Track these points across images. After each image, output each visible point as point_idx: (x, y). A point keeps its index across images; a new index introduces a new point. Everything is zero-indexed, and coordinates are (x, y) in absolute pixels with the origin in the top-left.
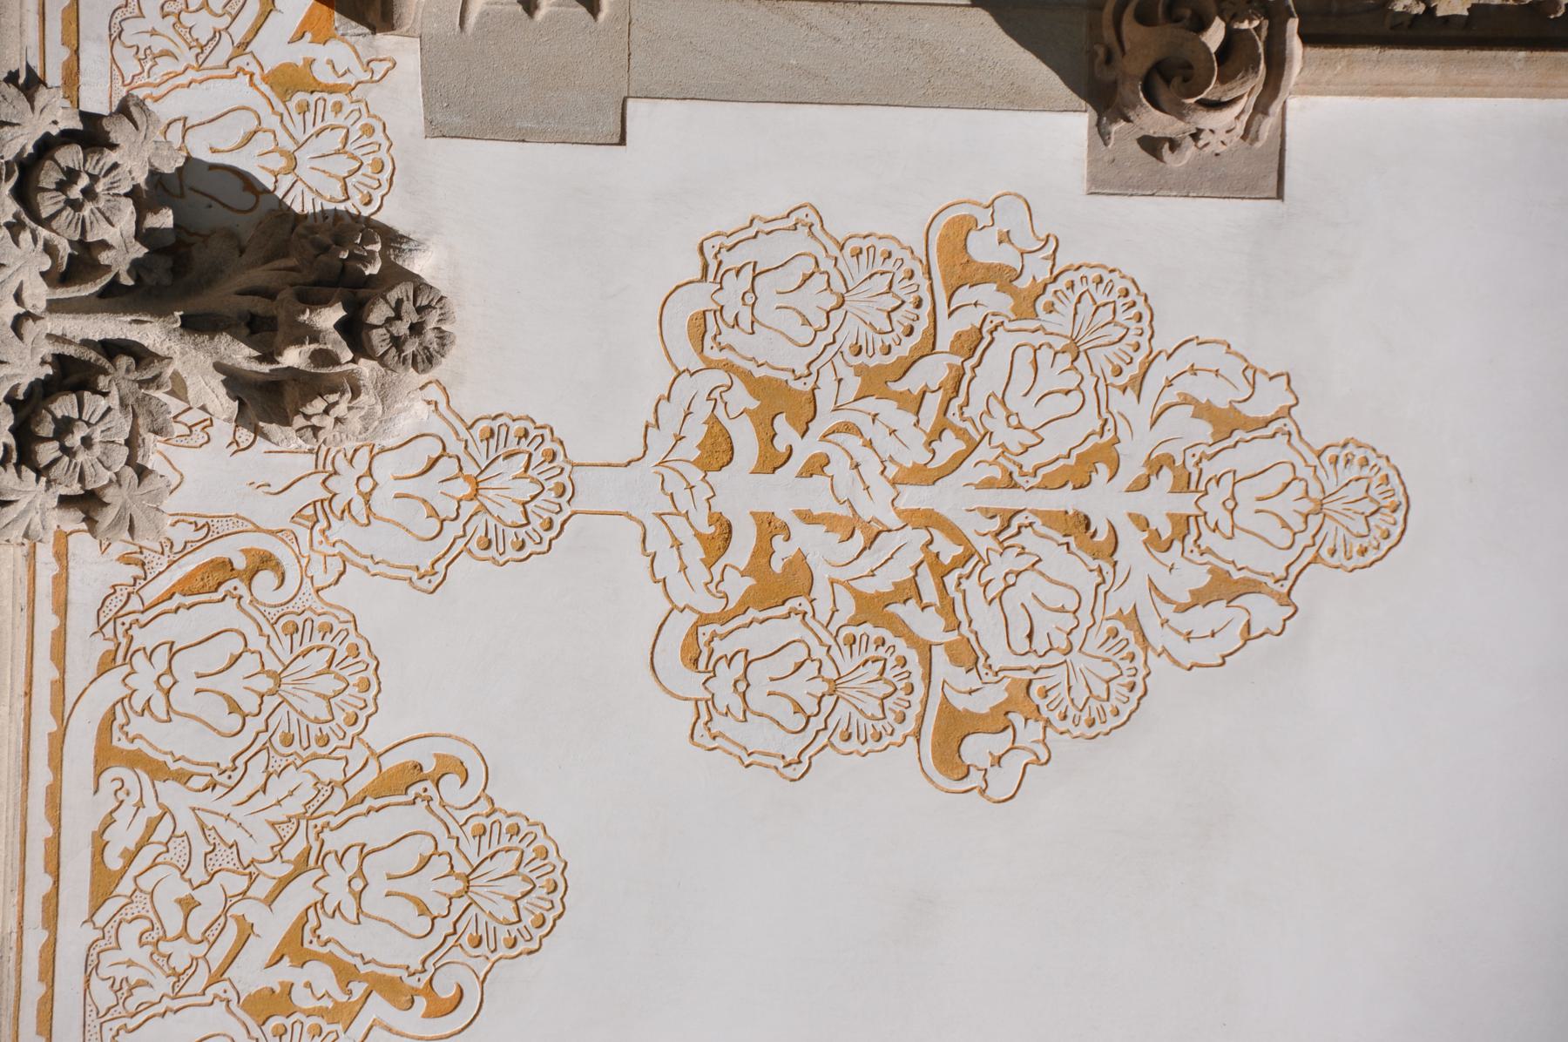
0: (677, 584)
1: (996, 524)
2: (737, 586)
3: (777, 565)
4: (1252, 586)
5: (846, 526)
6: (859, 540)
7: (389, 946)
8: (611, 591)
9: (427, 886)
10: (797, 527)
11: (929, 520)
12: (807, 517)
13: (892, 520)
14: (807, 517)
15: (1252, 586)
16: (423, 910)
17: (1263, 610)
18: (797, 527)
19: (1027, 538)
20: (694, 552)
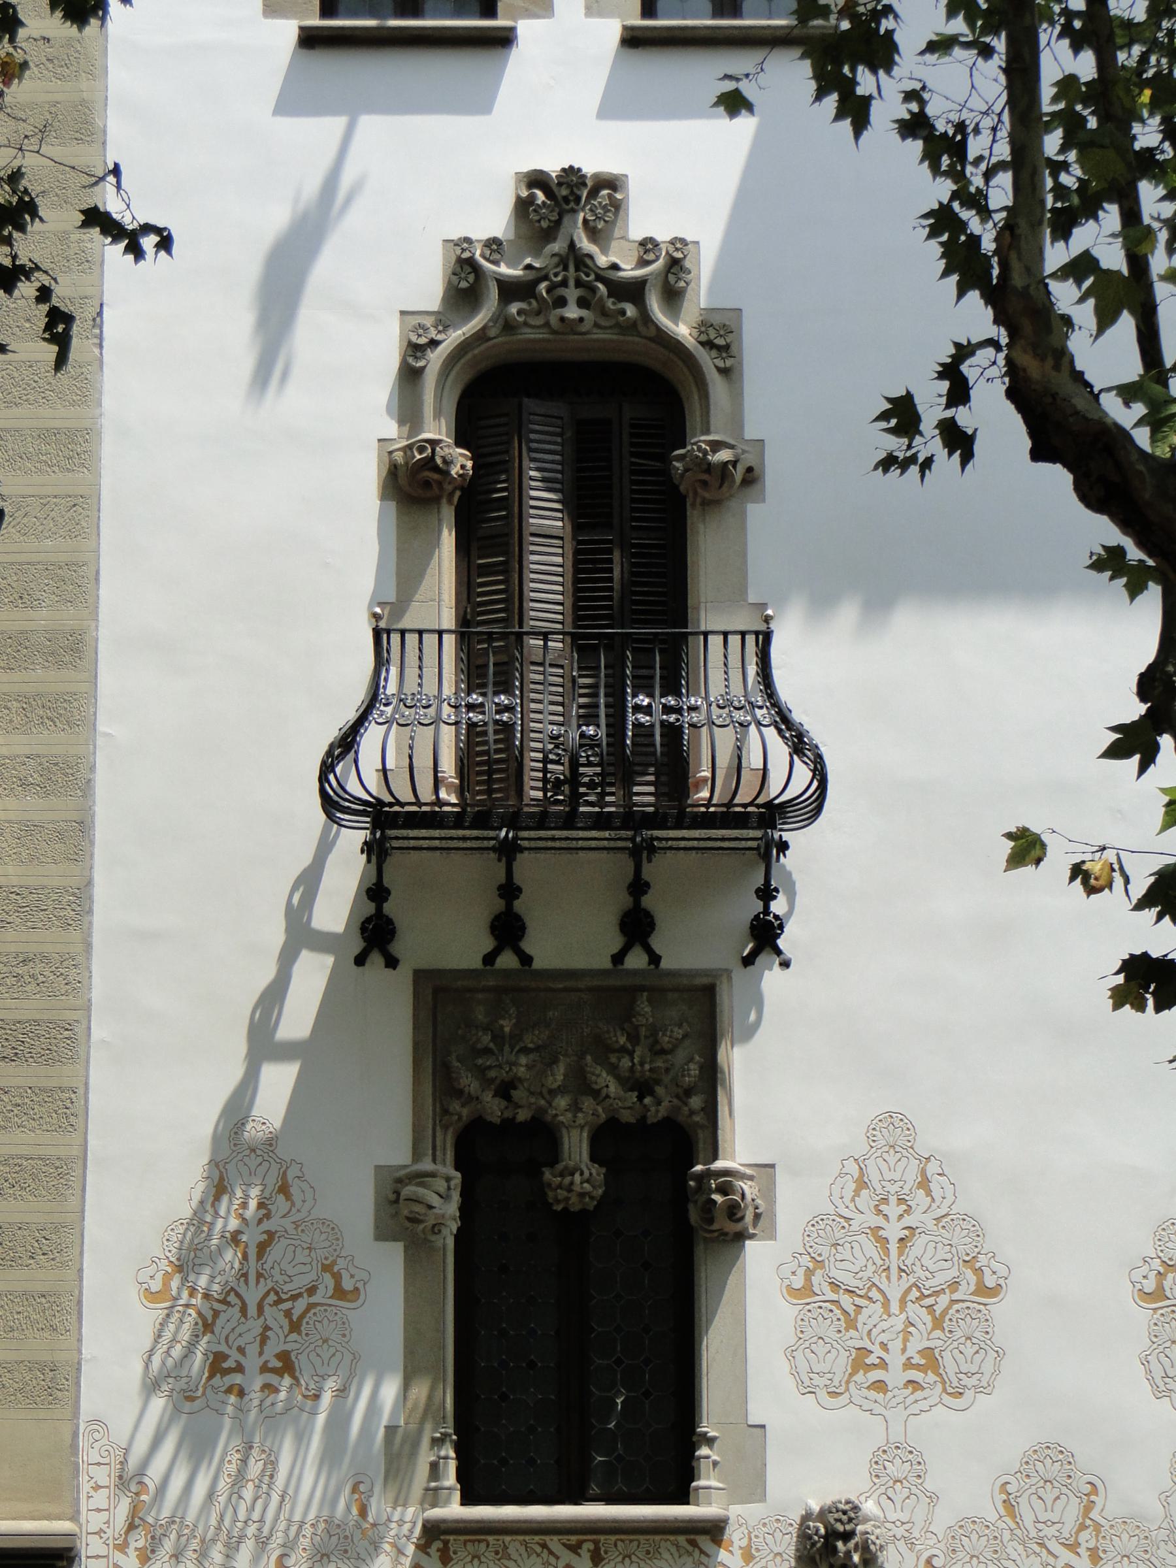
0: (931, 1401)
1: (903, 1274)
2: (931, 1377)
3: (923, 1362)
4: (923, 1172)
5: (906, 1335)
6: (911, 1329)
7: (1072, 1512)
8: (936, 1425)
9: (1049, 1497)
10: (908, 1354)
11: (903, 1302)
12: (904, 1350)
13: (903, 1316)
14: (904, 1350)
15: (923, 1172)
16: (1058, 1498)
17: (932, 1168)
18: (908, 1354)
19: (908, 1262)
20: (919, 1394)
